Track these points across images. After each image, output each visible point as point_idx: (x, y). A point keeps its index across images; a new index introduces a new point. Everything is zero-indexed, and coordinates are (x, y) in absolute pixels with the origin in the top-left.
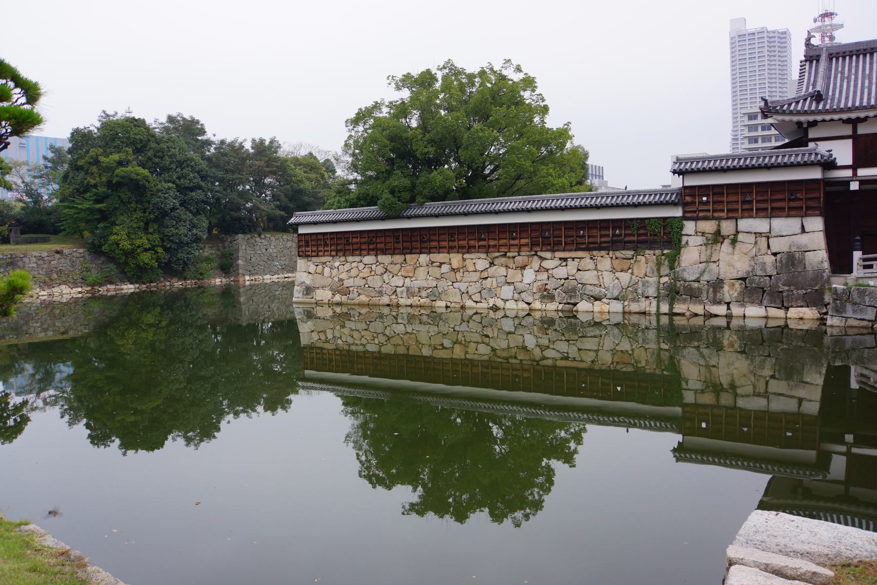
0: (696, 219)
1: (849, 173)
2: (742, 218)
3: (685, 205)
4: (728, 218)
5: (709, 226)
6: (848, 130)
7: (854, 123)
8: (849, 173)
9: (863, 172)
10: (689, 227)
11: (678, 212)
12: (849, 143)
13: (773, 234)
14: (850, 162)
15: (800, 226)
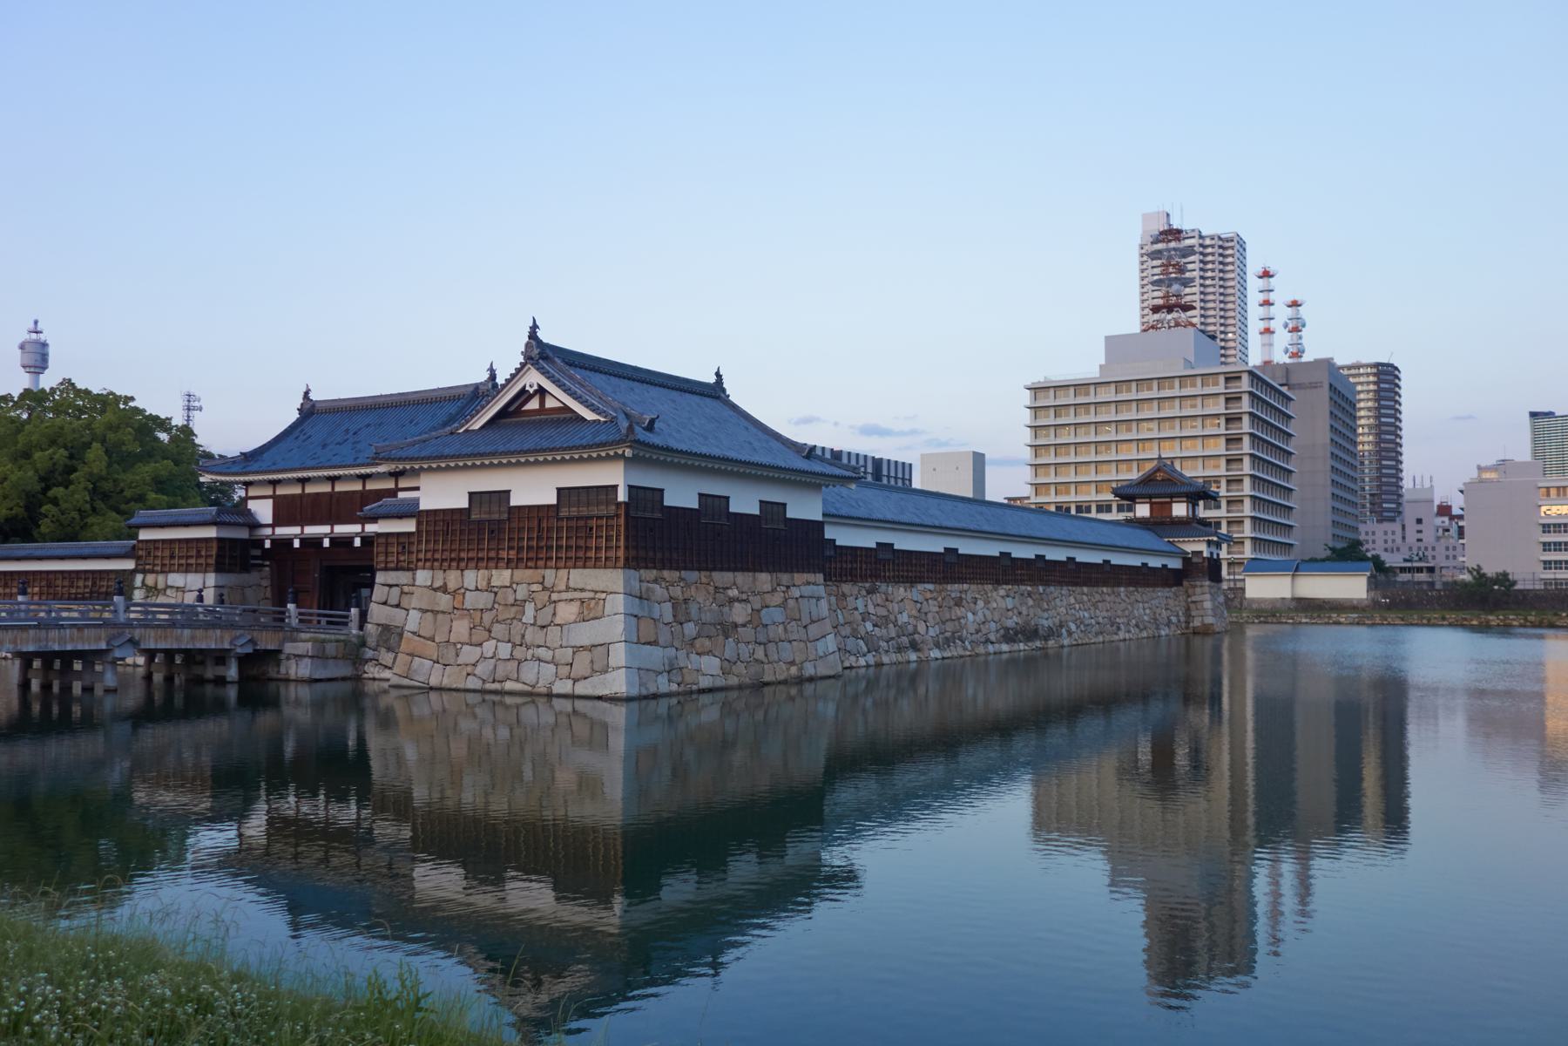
0: (144, 572)
1: (268, 531)
2: (170, 572)
3: (138, 558)
4: (162, 572)
5: (150, 579)
6: (269, 492)
7: (274, 483)
8: (268, 531)
9: (282, 531)
10: (139, 578)
11: (129, 565)
12: (270, 502)
13: (187, 589)
14: (269, 521)
15: (202, 582)
